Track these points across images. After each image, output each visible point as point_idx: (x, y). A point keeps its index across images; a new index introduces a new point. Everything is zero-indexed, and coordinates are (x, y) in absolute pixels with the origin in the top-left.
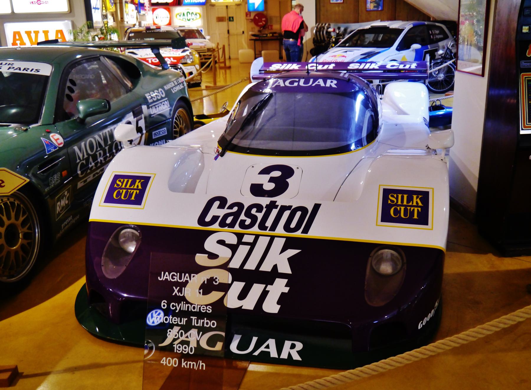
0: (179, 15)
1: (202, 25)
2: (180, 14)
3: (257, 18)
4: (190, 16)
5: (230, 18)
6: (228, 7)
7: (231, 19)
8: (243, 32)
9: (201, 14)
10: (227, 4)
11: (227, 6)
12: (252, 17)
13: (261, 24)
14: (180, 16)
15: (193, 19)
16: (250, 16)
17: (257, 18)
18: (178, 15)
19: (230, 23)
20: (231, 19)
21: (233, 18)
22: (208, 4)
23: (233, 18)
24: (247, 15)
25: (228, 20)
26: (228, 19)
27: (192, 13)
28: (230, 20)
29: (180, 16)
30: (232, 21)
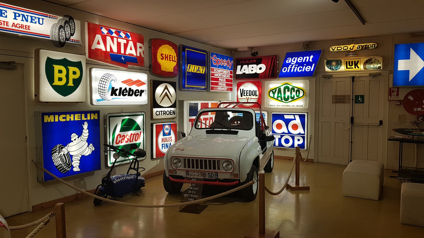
0: (273, 92)
1: (308, 107)
2: (274, 91)
3: (411, 98)
4: (288, 94)
5: (357, 97)
6: (355, 79)
7: (360, 99)
8: (381, 123)
9: (307, 91)
10: (353, 75)
11: (353, 78)
12: (401, 97)
13: (419, 109)
14: (274, 93)
15: (292, 98)
16: (398, 94)
17: (411, 98)
18: (271, 92)
19: (357, 106)
20: (360, 99)
21: (362, 97)
22: (320, 76)
23: (362, 97)
24: (390, 92)
25: (354, 101)
26: (353, 99)
27: (293, 89)
28: (357, 101)
29: (274, 93)
30: (361, 103)
